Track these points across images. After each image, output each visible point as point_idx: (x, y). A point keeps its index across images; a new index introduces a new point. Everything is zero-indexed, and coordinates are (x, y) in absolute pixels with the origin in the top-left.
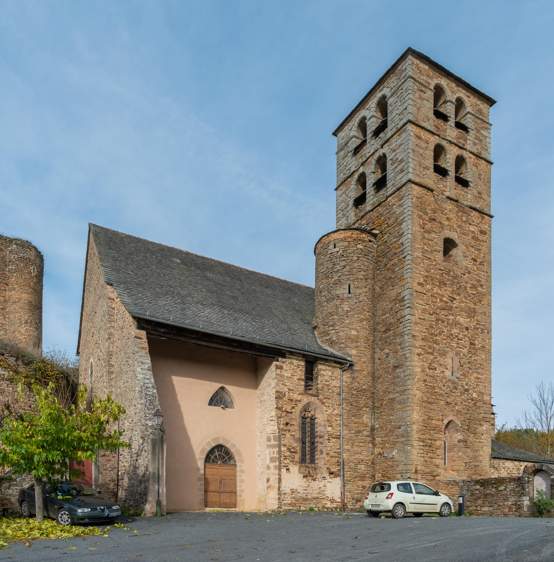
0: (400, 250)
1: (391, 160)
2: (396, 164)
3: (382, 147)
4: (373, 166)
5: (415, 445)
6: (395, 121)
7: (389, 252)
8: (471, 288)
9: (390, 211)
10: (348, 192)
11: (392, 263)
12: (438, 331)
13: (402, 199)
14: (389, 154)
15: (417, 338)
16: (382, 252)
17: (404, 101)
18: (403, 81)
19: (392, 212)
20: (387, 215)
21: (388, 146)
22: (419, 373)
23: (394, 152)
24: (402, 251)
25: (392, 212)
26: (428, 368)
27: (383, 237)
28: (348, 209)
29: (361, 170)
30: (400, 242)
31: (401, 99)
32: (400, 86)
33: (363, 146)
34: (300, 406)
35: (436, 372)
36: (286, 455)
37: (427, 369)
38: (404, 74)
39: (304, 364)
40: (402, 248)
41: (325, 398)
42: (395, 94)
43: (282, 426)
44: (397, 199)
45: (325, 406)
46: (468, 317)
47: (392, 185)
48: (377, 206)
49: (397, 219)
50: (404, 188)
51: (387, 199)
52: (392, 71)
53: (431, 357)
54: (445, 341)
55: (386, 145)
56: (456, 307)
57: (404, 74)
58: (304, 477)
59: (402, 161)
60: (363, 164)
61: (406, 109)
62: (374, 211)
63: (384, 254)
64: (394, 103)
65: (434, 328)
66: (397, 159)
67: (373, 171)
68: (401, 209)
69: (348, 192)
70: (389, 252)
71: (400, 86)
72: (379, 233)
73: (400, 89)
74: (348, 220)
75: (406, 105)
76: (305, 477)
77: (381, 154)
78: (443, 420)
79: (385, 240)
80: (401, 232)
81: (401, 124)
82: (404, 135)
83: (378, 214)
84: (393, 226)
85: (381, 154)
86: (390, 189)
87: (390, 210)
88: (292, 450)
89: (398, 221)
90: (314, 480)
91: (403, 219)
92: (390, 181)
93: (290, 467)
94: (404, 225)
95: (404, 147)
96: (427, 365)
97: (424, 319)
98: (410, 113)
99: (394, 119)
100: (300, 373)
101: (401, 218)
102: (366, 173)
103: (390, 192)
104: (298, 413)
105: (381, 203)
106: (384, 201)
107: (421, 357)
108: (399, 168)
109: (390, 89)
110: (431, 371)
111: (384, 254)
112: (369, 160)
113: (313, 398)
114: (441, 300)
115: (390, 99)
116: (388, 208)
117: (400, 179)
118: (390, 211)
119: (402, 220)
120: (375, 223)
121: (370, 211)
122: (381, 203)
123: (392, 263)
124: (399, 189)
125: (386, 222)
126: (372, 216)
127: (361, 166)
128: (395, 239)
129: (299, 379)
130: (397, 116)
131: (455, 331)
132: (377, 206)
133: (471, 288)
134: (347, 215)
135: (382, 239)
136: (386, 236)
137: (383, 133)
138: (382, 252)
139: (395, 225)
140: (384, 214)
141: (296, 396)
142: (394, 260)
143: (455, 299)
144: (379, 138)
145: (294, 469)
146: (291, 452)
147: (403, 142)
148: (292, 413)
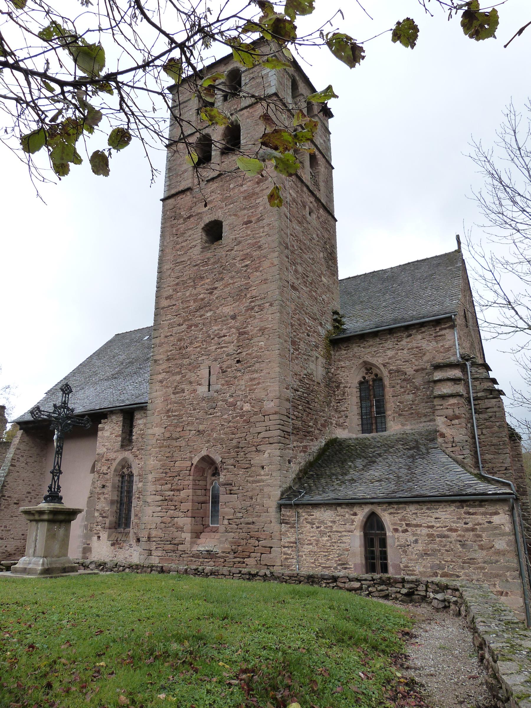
5: (149, 500)
12: (189, 341)
22: (160, 404)
26: (174, 393)
34: (115, 464)
35: (184, 394)
36: (98, 520)
37: (172, 396)
39: (121, 419)
41: (138, 450)
43: (98, 490)
45: (138, 459)
46: (235, 301)
53: (178, 377)
54: (198, 349)
56: (217, 298)
58: (113, 545)
65: (184, 339)
76: (113, 545)
78: (191, 458)
88: (104, 515)
90: (121, 548)
93: (101, 535)
96: (170, 390)
97: (171, 335)
100: (117, 429)
104: (112, 472)
107: (164, 383)
110: (177, 395)
113: (126, 453)
114: (195, 301)
129: (116, 436)
131: (215, 328)
141: (112, 455)
143: (216, 288)
145: (104, 535)
146: (103, 517)
148: (107, 473)
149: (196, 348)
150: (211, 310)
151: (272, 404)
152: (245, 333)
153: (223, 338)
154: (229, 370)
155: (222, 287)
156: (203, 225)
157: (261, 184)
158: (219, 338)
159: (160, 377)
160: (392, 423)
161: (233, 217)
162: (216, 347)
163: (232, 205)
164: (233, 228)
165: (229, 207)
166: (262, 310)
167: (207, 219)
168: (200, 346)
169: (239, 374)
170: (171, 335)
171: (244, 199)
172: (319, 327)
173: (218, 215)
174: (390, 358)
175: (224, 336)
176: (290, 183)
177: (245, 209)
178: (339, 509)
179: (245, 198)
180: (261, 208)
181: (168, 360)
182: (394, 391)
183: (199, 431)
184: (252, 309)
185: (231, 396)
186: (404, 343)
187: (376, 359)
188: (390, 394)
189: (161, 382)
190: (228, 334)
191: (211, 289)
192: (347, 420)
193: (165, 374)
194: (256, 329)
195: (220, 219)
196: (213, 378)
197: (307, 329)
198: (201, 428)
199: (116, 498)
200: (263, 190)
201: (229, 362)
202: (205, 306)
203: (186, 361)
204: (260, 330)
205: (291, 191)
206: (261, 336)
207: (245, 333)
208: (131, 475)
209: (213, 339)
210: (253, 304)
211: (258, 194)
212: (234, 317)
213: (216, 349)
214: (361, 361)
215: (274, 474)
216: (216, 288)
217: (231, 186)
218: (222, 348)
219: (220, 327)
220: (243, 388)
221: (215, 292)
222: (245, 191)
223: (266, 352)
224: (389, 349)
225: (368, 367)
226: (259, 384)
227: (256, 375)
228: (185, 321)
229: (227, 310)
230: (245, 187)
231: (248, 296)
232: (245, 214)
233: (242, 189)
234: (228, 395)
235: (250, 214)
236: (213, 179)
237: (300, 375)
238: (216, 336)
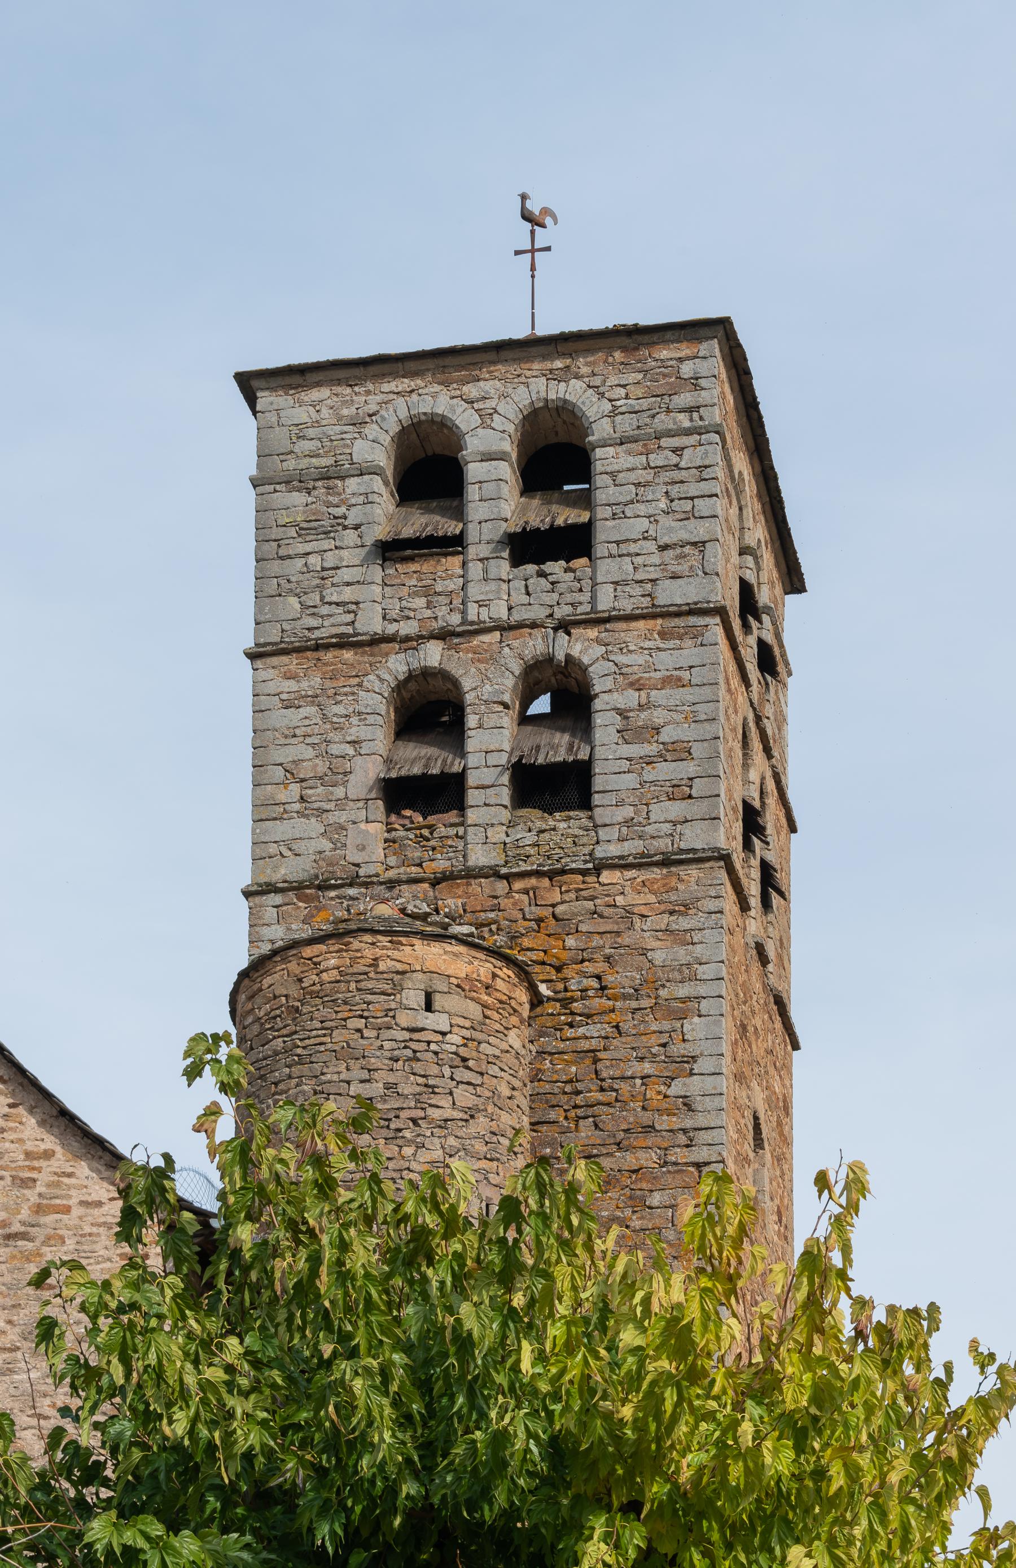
0: (675, 1122)
1: (621, 713)
2: (652, 749)
3: (565, 626)
4: (510, 682)
6: (639, 560)
7: (608, 1104)
9: (618, 933)
10: (340, 709)
11: (630, 1160)
13: (680, 913)
14: (609, 683)
16: (568, 1088)
17: (687, 506)
18: (684, 421)
19: (626, 939)
20: (596, 941)
21: (598, 641)
23: (637, 686)
24: (684, 1131)
25: (626, 939)
27: (571, 1025)
28: (339, 792)
29: (433, 654)
30: (676, 1088)
31: (675, 491)
32: (670, 434)
33: (446, 555)
38: (685, 399)
40: (689, 1124)
42: (638, 447)
44: (652, 899)
47: (628, 822)
48: (538, 874)
49: (655, 984)
50: (693, 872)
51: (598, 870)
52: (626, 341)
55: (592, 633)
57: (685, 399)
59: (679, 751)
60: (444, 635)
61: (699, 545)
62: (518, 885)
63: (579, 1100)
64: (633, 477)
66: (657, 730)
67: (507, 698)
68: (682, 954)
69: (340, 709)
70: (608, 1104)
71: (670, 434)
72: (549, 999)
73: (665, 442)
74: (339, 845)
75: (699, 530)
77: (560, 656)
79: (585, 1045)
80: (677, 1049)
81: (672, 594)
82: (689, 653)
83: (547, 912)
84: (634, 1004)
85: (560, 656)
86: (613, 833)
87: (615, 928)
89: (663, 993)
91: (689, 999)
92: (611, 799)
94: (694, 1027)
95: (691, 698)
98: (717, 574)
99: (633, 548)
101: (683, 991)
102: (467, 684)
103: (613, 850)
105: (563, 872)
106: (584, 873)
108: (664, 771)
109: (607, 407)
111: (579, 1100)
112: (486, 638)
115: (611, 450)
116: (608, 911)
117: (675, 823)
118: (618, 933)
119: (684, 1000)
120: (526, 942)
121: (493, 873)
122: (563, 872)
123: (630, 1160)
124: (666, 862)
125: (589, 968)
126: (504, 902)
127: (433, 636)
128: (647, 1068)
130: (651, 546)
132: (538, 874)
134: (332, 818)
135: (570, 1033)
136: (593, 1030)
137: (562, 563)
138: (568, 1088)
139: (645, 1003)
140: (583, 928)
142: (641, 1154)
144: (542, 574)
147: (685, 675)
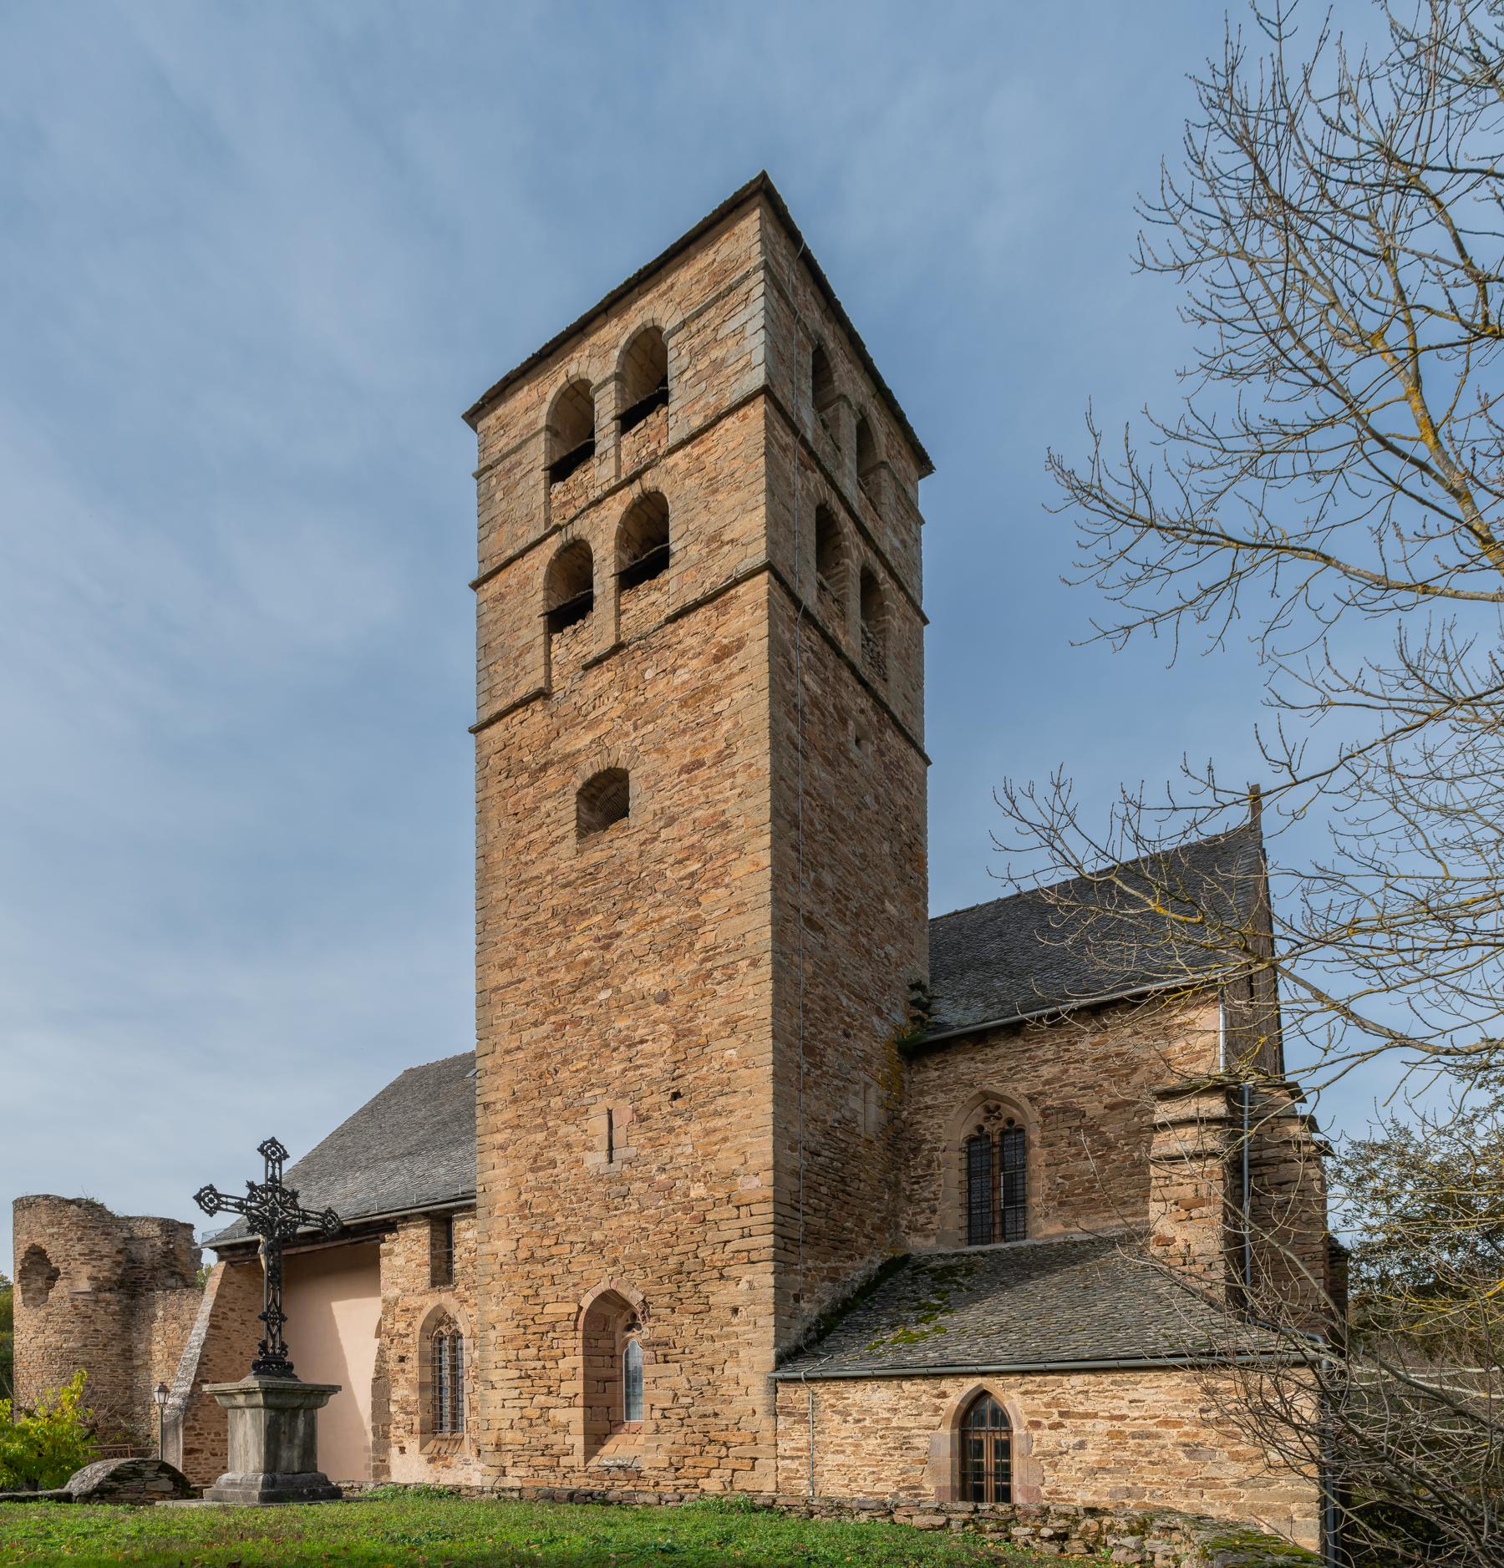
8: (680, 862)
15: (499, 1107)
26: (532, 1170)
53: (540, 1137)
56: (621, 957)
88: (409, 1409)
133: (680, 862)
143: (618, 934)
146: (407, 1413)
149: (577, 1071)
150: (607, 986)
151: (756, 1182)
152: (690, 1032)
153: (639, 1047)
154: (656, 1114)
155: (632, 931)
156: (579, 784)
157: (727, 661)
158: (629, 1047)
159: (499, 1138)
160: (1041, 1220)
161: (655, 756)
162: (622, 1066)
163: (650, 727)
164: (655, 787)
165: (644, 731)
166: (730, 977)
167: (588, 769)
168: (585, 1068)
169: (679, 1122)
170: (519, 1048)
171: (682, 707)
172: (875, 1019)
173: (619, 755)
174: (1047, 1082)
175: (642, 1042)
176: (805, 656)
177: (684, 731)
178: (906, 1385)
179: (684, 703)
180: (727, 725)
181: (514, 1101)
182: (1051, 1154)
183: (592, 1244)
184: (709, 974)
185: (662, 1170)
186: (1085, 1045)
187: (1011, 1085)
188: (1041, 1161)
189: (502, 1148)
190: (650, 1037)
191: (605, 937)
192: (935, 1218)
193: (510, 1131)
194: (717, 1021)
195: (622, 765)
196: (619, 1135)
197: (842, 1021)
198: (597, 1236)
199: (429, 1379)
200: (730, 677)
201: (656, 1098)
202: (593, 979)
203: (556, 1102)
204: (727, 1022)
205: (807, 679)
206: (729, 1037)
207: (690, 1032)
208: (456, 1336)
209: (614, 1050)
210: (709, 965)
211: (717, 688)
212: (664, 999)
213: (625, 1070)
214: (975, 1092)
215: (761, 1322)
216: (618, 934)
217: (649, 675)
218: (638, 1067)
219: (629, 1022)
220: (689, 1150)
221: (618, 942)
222: (684, 683)
223: (743, 1072)
224: (1046, 1062)
225: (992, 1105)
226: (725, 1140)
227: (719, 1122)
228: (547, 1014)
229: (649, 982)
230: (682, 676)
231: (698, 946)
232: (681, 750)
233: (677, 681)
234: (654, 1167)
235: (700, 743)
236: (598, 661)
237: (825, 1122)
238: (622, 1042)
